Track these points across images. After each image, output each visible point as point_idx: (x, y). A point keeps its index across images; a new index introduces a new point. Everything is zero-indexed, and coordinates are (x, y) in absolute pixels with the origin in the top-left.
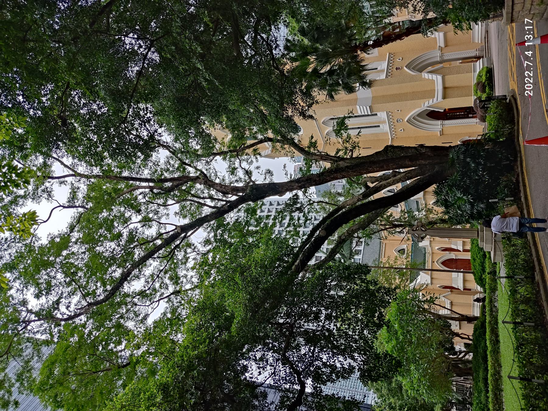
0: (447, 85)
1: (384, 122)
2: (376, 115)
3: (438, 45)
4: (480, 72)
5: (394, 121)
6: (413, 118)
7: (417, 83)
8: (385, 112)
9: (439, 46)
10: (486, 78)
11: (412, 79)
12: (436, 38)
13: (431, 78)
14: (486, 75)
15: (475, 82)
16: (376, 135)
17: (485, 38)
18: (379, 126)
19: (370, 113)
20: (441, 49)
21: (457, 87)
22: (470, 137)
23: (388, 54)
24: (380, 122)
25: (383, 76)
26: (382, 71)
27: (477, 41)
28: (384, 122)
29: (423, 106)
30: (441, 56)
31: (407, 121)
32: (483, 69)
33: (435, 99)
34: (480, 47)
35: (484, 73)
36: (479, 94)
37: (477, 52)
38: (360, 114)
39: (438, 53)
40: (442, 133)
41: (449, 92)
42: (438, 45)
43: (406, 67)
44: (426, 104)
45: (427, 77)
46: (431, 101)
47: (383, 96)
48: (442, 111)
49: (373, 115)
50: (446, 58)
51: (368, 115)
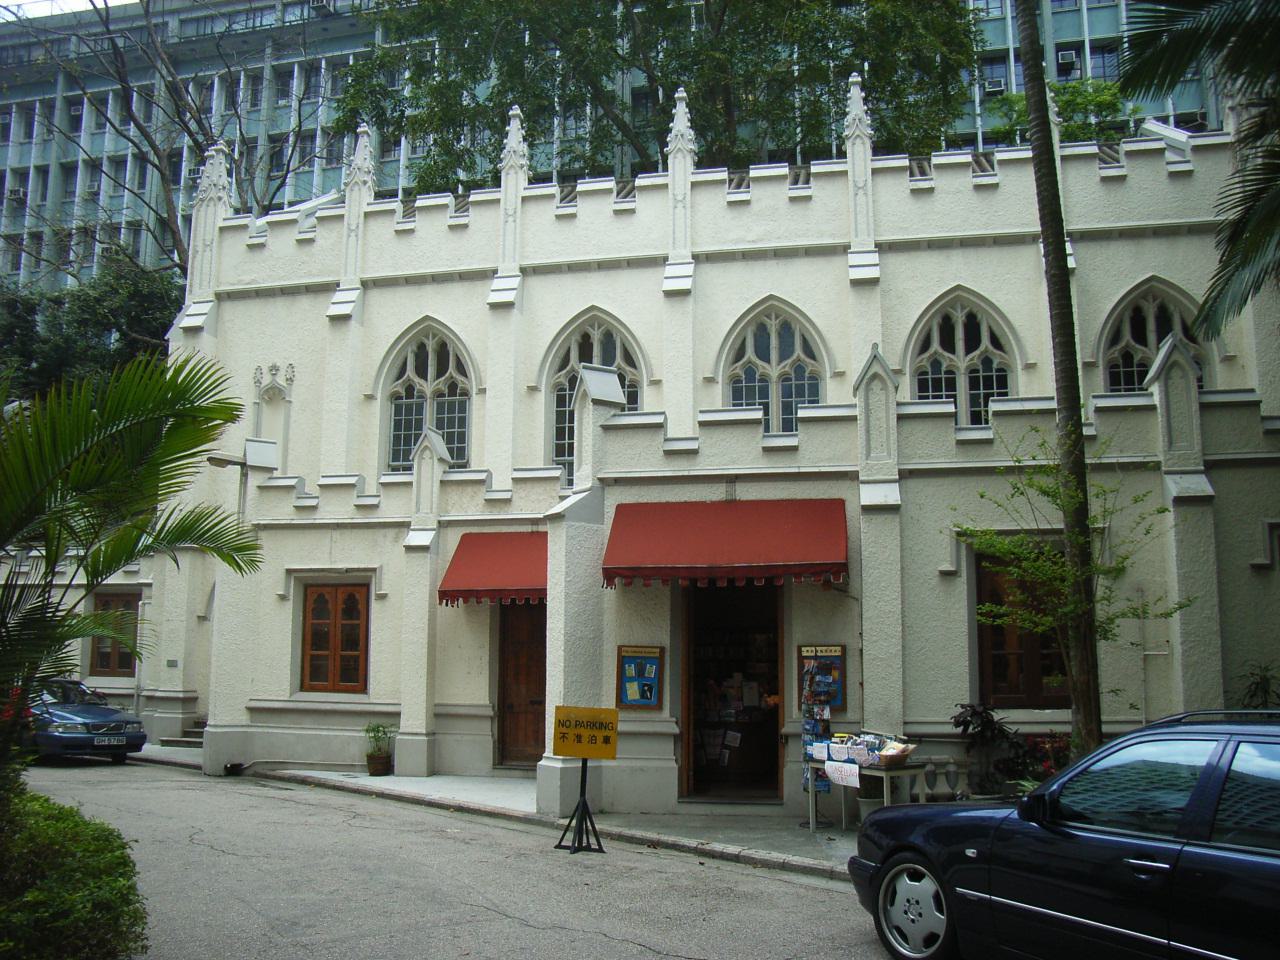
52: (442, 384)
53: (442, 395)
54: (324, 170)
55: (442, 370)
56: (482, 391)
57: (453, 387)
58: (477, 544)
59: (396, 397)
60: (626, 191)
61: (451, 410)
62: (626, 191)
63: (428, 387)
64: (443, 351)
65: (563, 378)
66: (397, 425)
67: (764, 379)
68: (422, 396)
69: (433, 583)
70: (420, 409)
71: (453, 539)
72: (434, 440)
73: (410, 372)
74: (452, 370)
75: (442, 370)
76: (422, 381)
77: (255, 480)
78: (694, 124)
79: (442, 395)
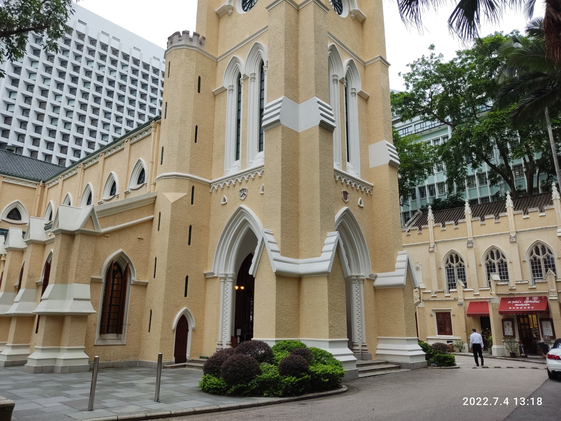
0: (306, 284)
1: (244, 165)
2: (260, 149)
3: (379, 274)
4: (330, 356)
5: (244, 183)
6: (245, 222)
7: (318, 220)
8: (263, 164)
9: (376, 277)
10: (319, 376)
11: (327, 212)
12: (393, 269)
13: (325, 248)
14: (326, 375)
15: (309, 345)
16: (222, 155)
17: (387, 363)
18: (237, 158)
19: (264, 124)
20: (371, 279)
21: (299, 305)
22: (194, 330)
23: (372, 184)
24: (244, 156)
25: (336, 167)
26: (344, 167)
27: (380, 346)
28: (244, 165)
29: (266, 230)
30: (358, 279)
31: (241, 208)
32: (338, 364)
33: (278, 256)
34: (370, 352)
35: (329, 368)
36: (281, 356)
37: (359, 348)
38: (266, 105)
39: (364, 273)
40: (208, 278)
41: (291, 287)
42: (379, 274)
43: (347, 211)
44: (268, 237)
45: (327, 240)
46: (276, 247)
47: (297, 154)
48: (250, 272)
49: (261, 143)
50: (354, 287)
51: (261, 122)
52: (457, 264)
53: (458, 267)
54: (411, 202)
55: (457, 261)
56: (468, 266)
57: (461, 265)
58: (473, 304)
59: (447, 268)
60: (497, 217)
61: (461, 270)
62: (497, 217)
63: (455, 265)
64: (457, 257)
65: (487, 262)
66: (448, 274)
67: (539, 260)
68: (453, 267)
69: (465, 313)
70: (453, 270)
71: (468, 304)
72: (460, 283)
73: (450, 262)
74: (460, 261)
75: (457, 261)
76: (453, 264)
77: (422, 291)
78: (512, 199)
79: (458, 267)
